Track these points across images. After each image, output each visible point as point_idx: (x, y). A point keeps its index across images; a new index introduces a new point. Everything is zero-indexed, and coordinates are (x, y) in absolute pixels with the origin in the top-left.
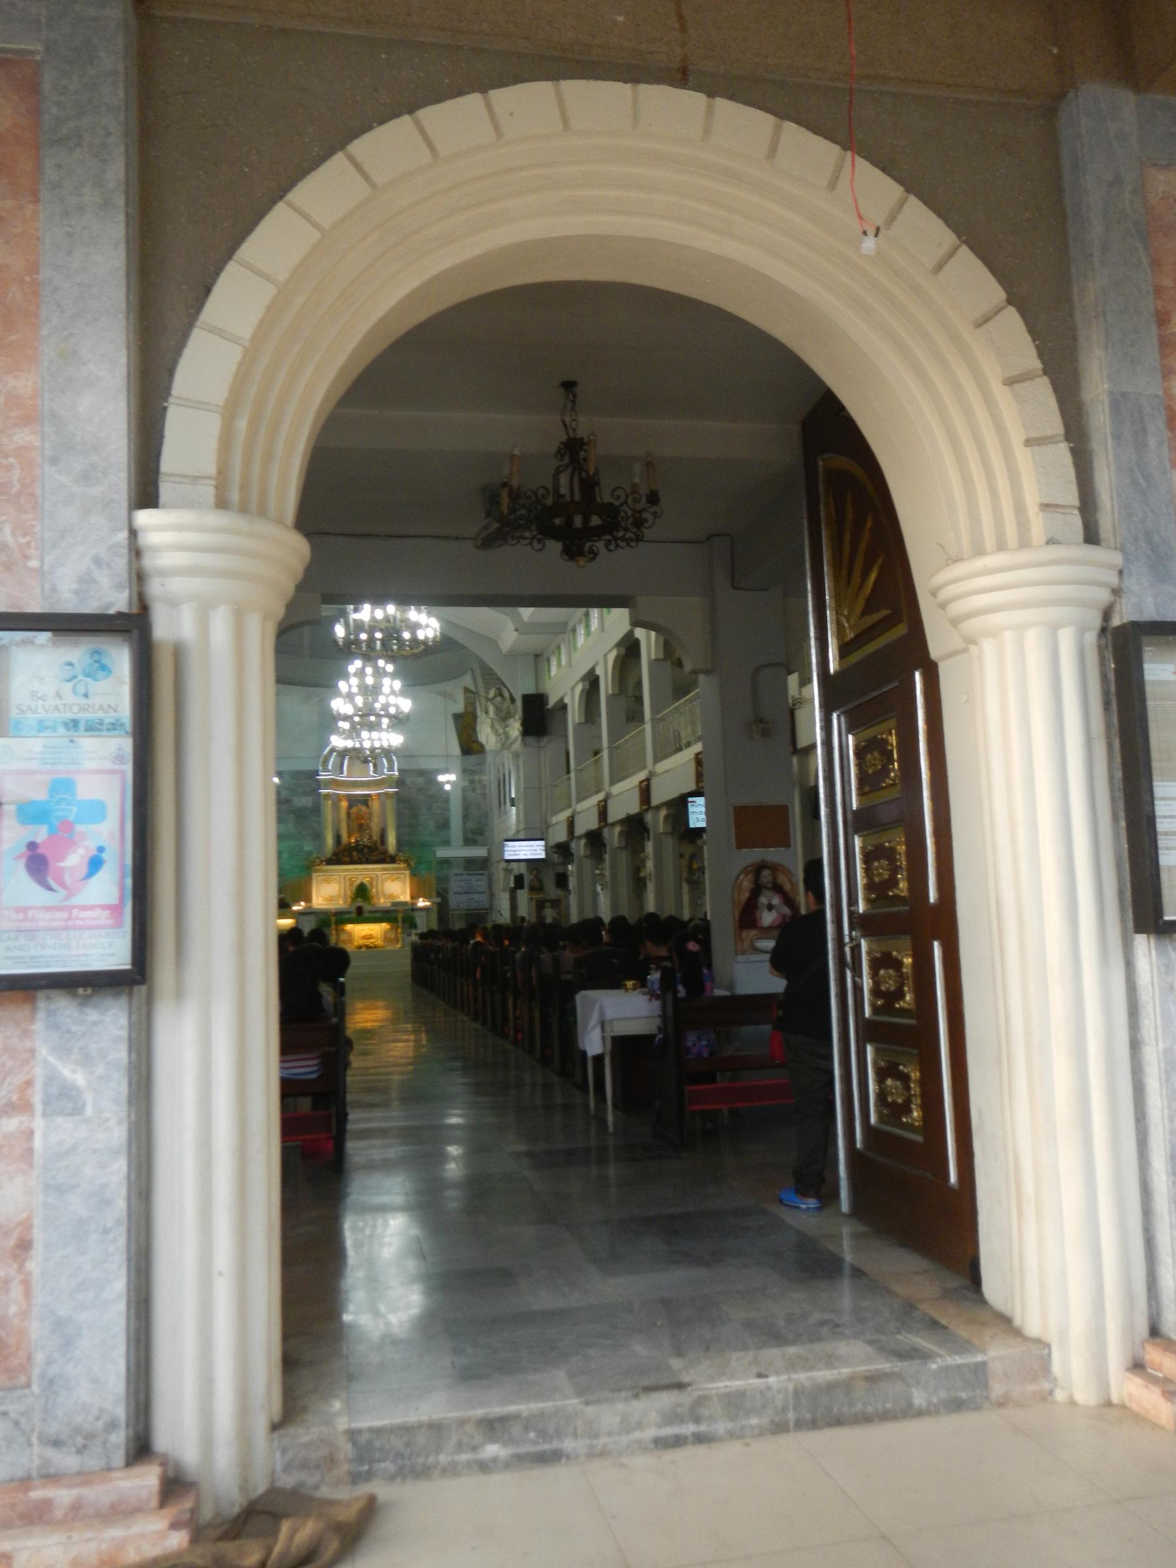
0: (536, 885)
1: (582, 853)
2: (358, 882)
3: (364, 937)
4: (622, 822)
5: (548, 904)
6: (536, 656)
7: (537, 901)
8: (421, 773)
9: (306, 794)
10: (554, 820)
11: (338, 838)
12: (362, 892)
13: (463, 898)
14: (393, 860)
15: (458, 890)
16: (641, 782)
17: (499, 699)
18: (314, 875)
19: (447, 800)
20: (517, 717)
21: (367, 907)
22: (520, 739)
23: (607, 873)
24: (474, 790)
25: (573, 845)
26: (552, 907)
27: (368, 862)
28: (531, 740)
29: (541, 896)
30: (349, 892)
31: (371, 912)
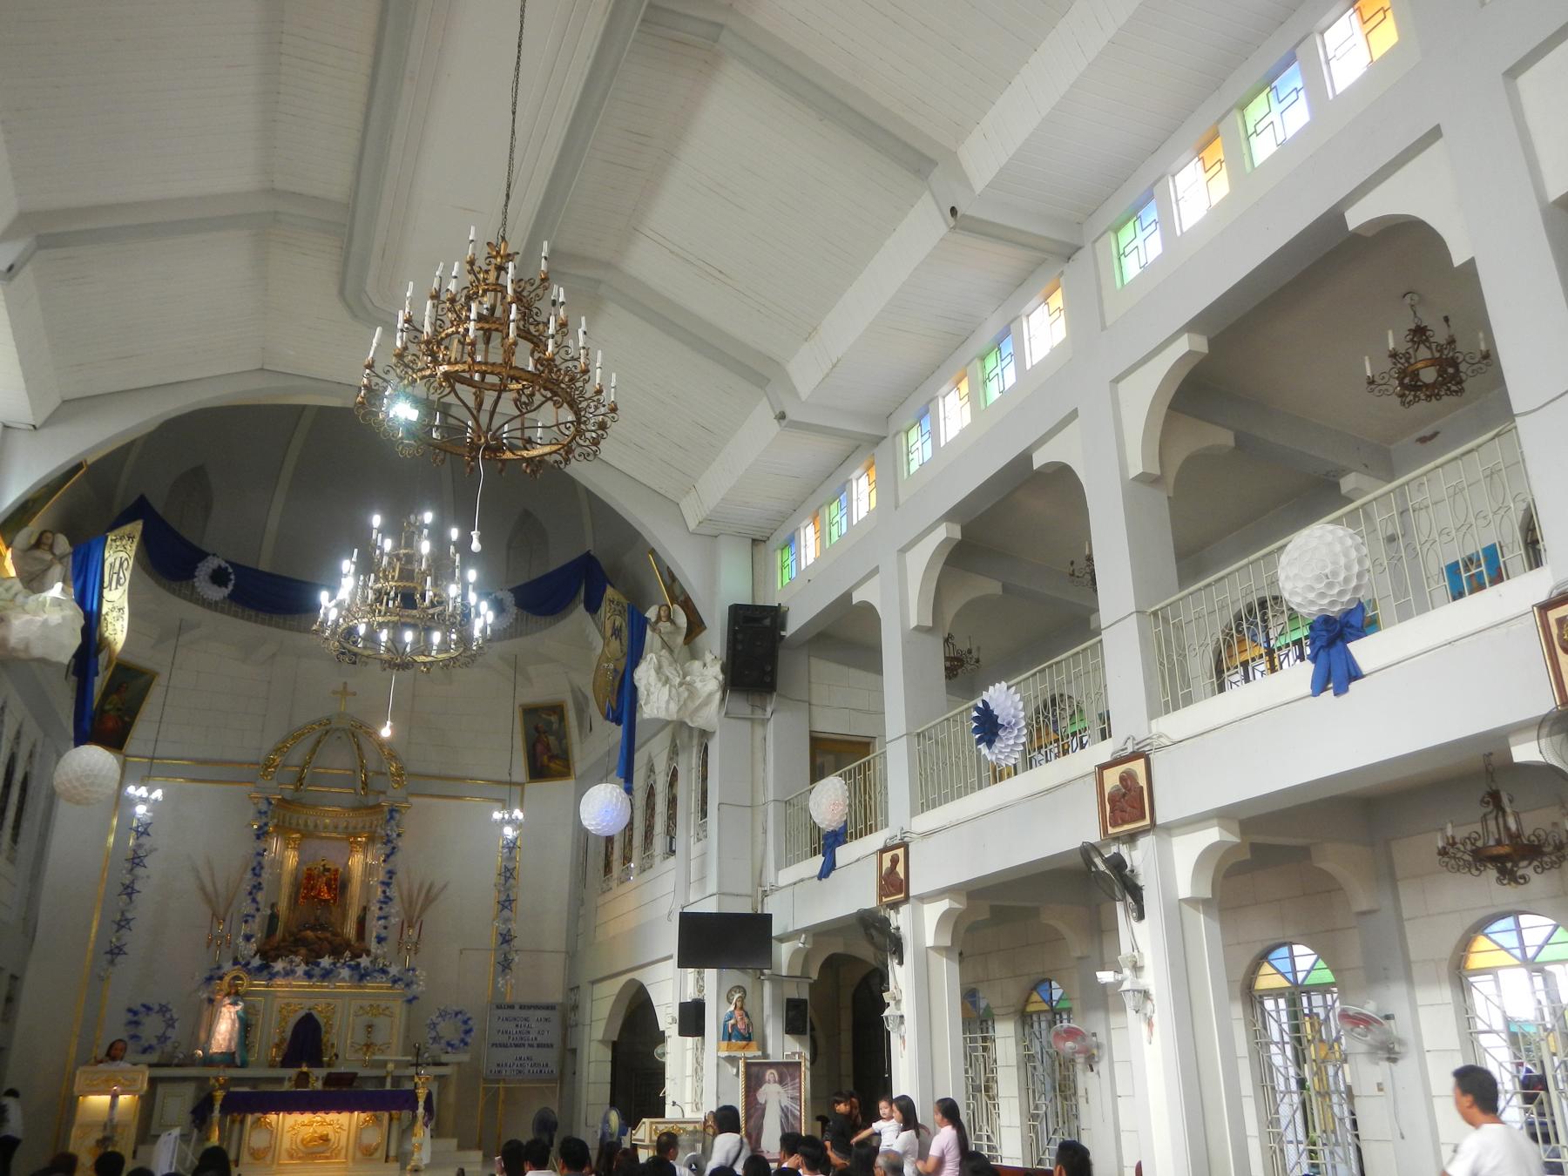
0: (740, 1026)
1: (930, 941)
2: (302, 1013)
4: (1223, 815)
5: (771, 1074)
6: (754, 541)
7: (747, 1065)
10: (788, 876)
15: (503, 1039)
16: (1545, 607)
17: (665, 626)
20: (709, 657)
22: (718, 696)
23: (1155, 978)
25: (901, 920)
26: (781, 1081)
28: (742, 706)
29: (753, 1053)
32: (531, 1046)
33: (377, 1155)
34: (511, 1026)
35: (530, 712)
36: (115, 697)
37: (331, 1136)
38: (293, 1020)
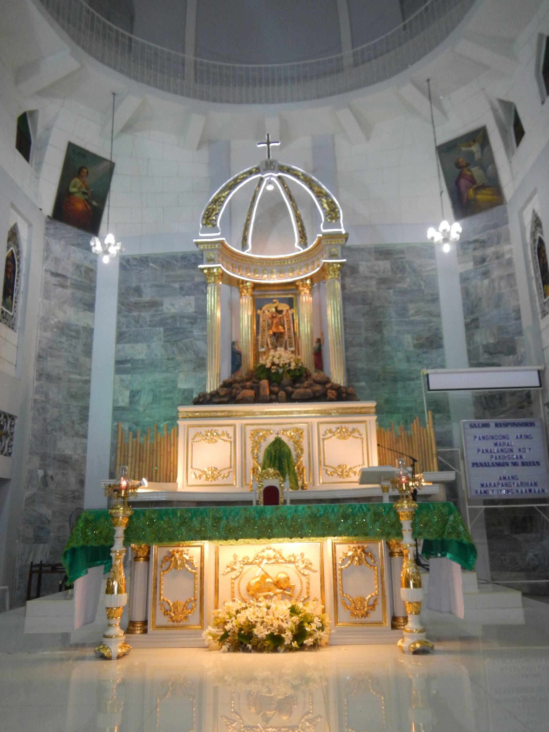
2: (271, 439)
3: (254, 592)
8: (384, 253)
9: (184, 292)
11: (236, 358)
12: (279, 457)
13: (493, 475)
14: (342, 395)
15: (485, 458)
18: (181, 423)
19: (435, 299)
21: (287, 492)
24: (486, 274)
27: (290, 399)
30: (251, 462)
31: (293, 502)
32: (515, 464)
33: (376, 615)
34: (489, 445)
35: (445, 151)
36: (76, 181)
37: (295, 581)
38: (265, 445)
